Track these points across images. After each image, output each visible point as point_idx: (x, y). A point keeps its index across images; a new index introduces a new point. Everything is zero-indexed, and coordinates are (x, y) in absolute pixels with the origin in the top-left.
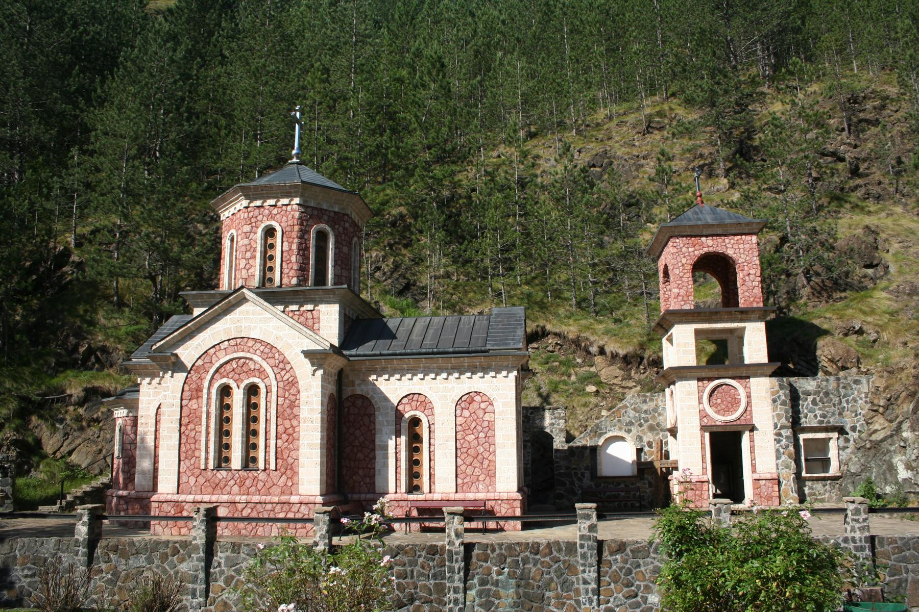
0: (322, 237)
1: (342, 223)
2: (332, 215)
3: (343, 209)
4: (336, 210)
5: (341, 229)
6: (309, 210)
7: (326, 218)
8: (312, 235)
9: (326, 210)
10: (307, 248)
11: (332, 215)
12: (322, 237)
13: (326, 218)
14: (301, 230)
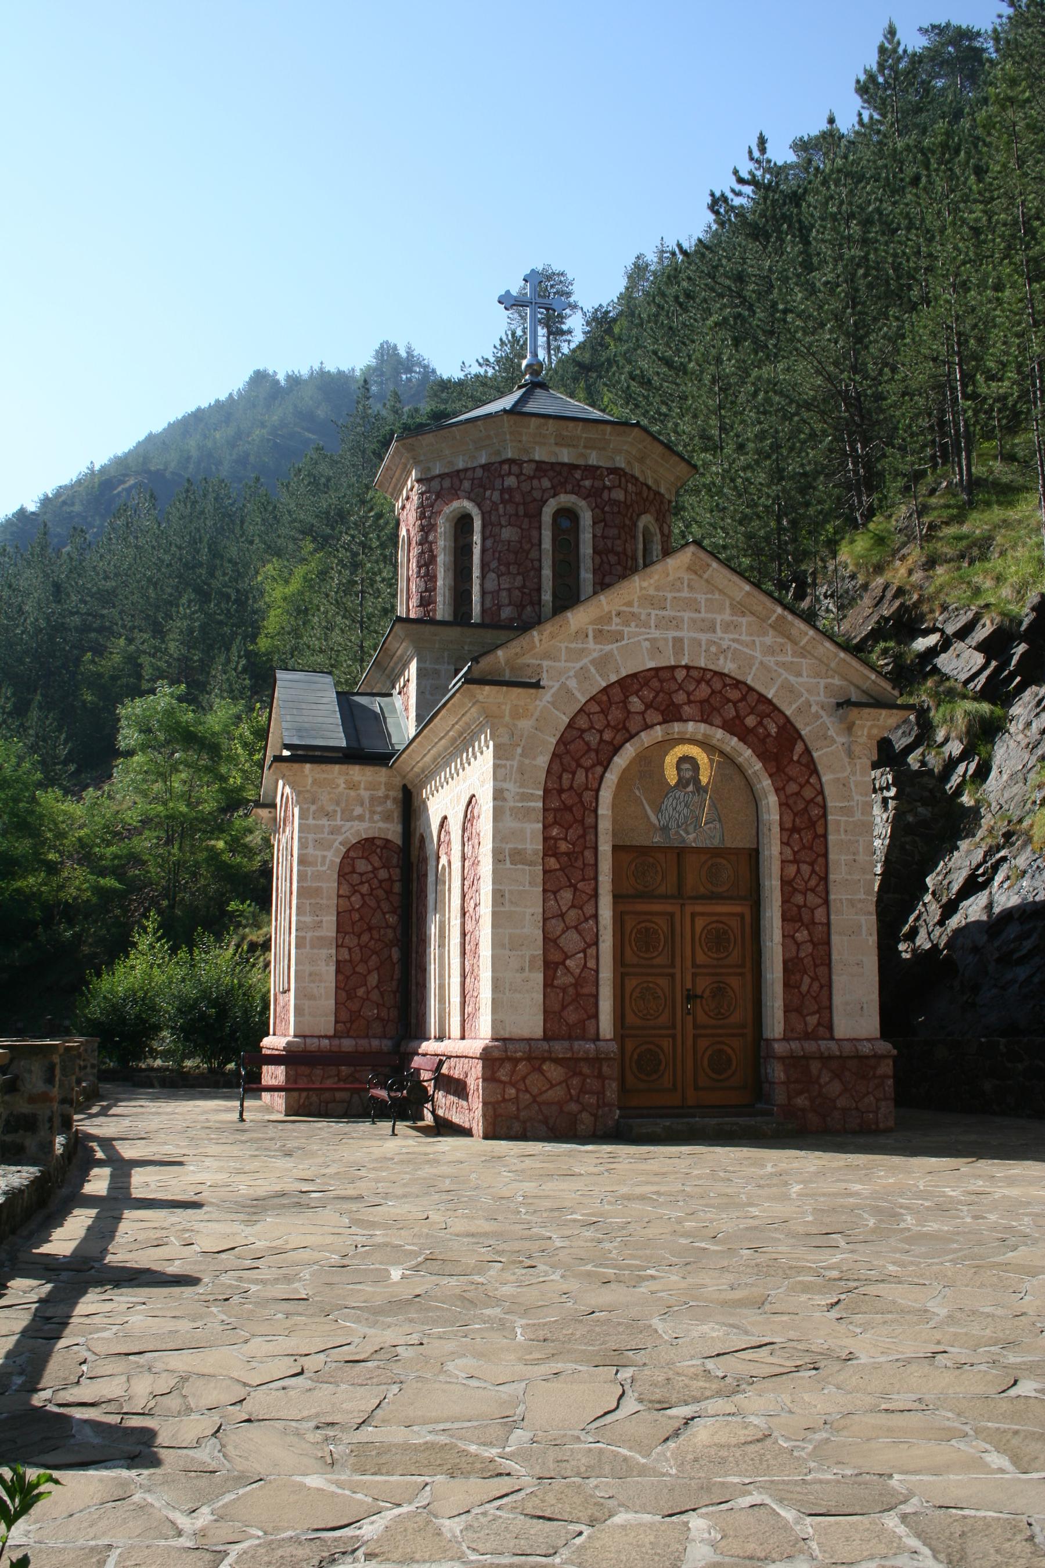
0: (463, 523)
1: (498, 483)
2: (479, 473)
3: (498, 453)
4: (483, 461)
5: (496, 496)
6: (435, 485)
7: (466, 484)
8: (443, 528)
9: (466, 470)
10: (433, 558)
11: (479, 473)
12: (462, 524)
13: (466, 484)
14: (422, 528)
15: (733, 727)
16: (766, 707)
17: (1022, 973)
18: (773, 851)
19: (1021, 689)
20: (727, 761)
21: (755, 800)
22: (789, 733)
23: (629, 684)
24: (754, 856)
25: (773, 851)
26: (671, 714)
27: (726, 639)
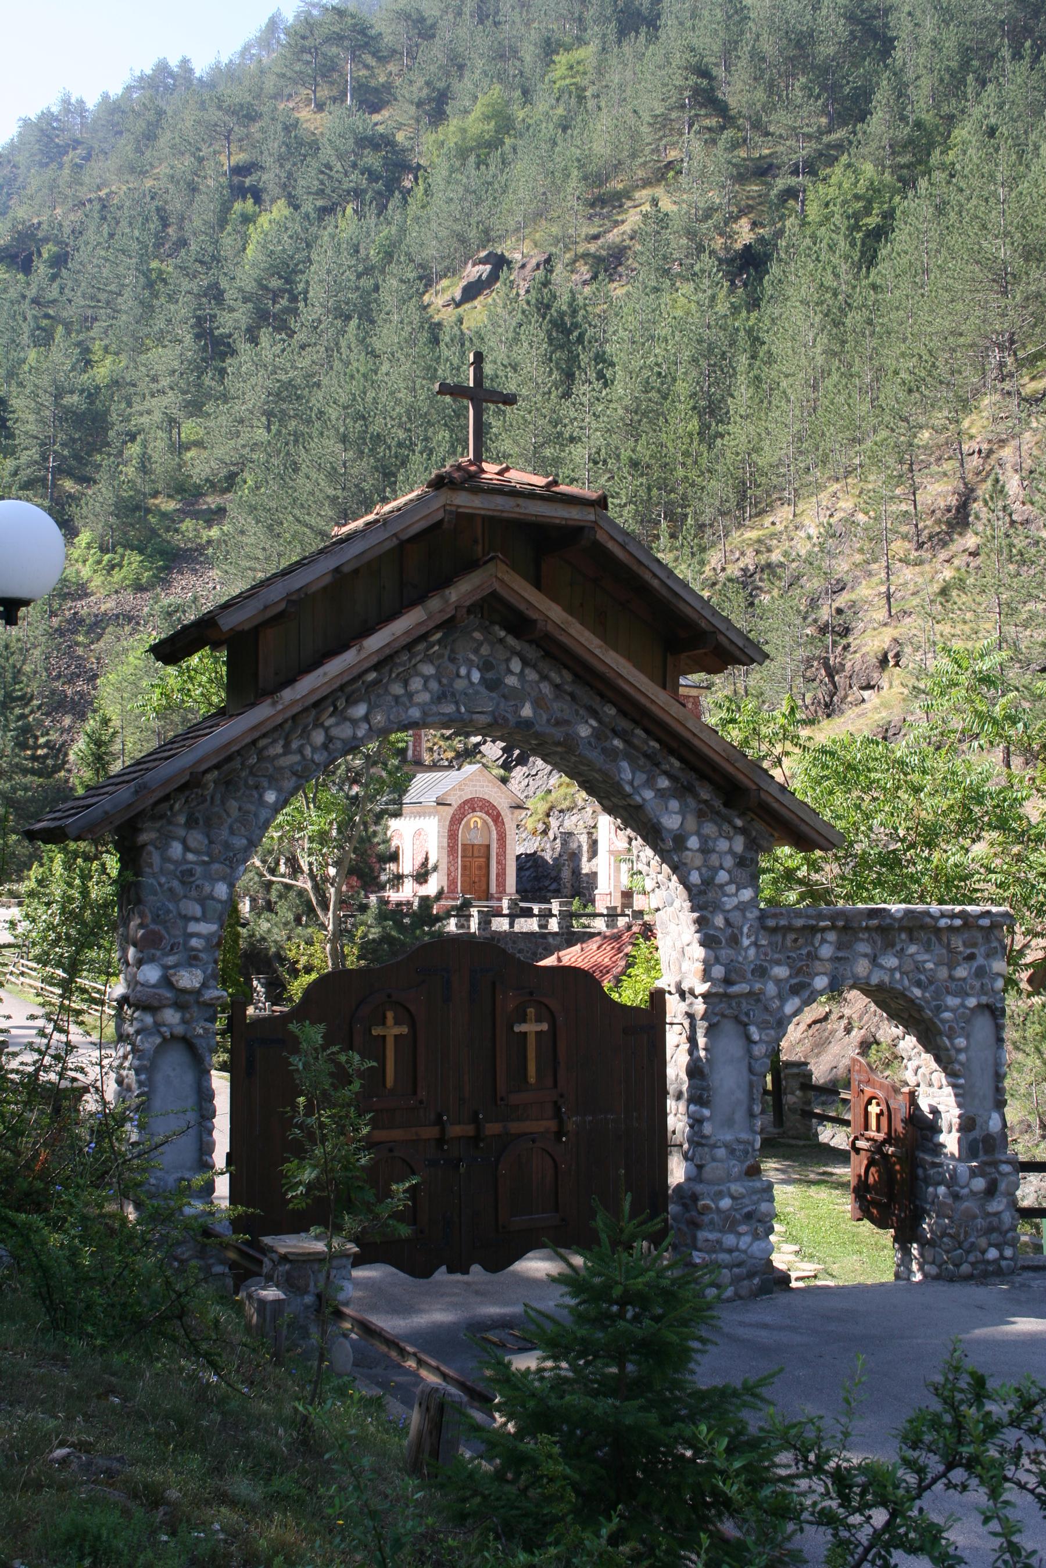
15: (487, 813)
16: (494, 807)
17: (527, 873)
18: (494, 846)
19: (515, 766)
20: (485, 822)
21: (490, 832)
22: (499, 814)
23: (465, 802)
24: (488, 847)
25: (494, 846)
26: (474, 810)
27: (486, 790)
